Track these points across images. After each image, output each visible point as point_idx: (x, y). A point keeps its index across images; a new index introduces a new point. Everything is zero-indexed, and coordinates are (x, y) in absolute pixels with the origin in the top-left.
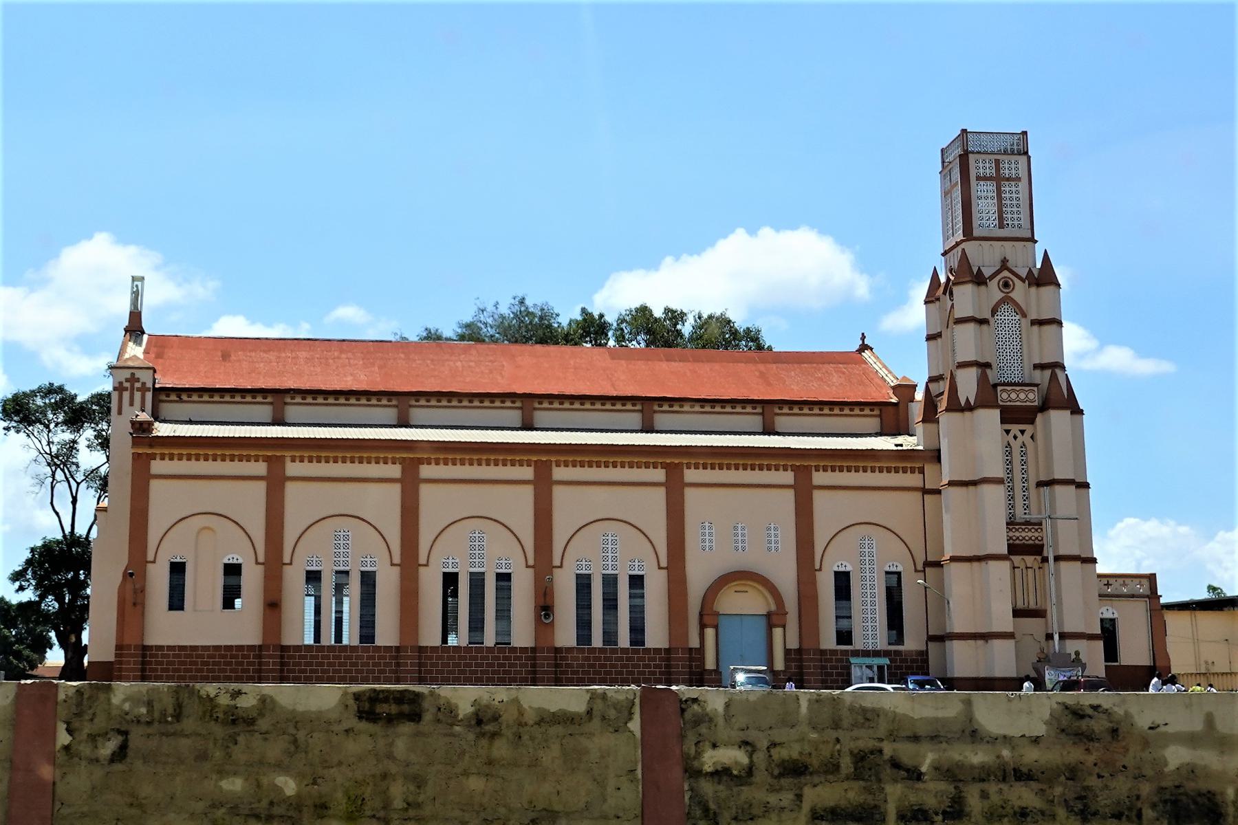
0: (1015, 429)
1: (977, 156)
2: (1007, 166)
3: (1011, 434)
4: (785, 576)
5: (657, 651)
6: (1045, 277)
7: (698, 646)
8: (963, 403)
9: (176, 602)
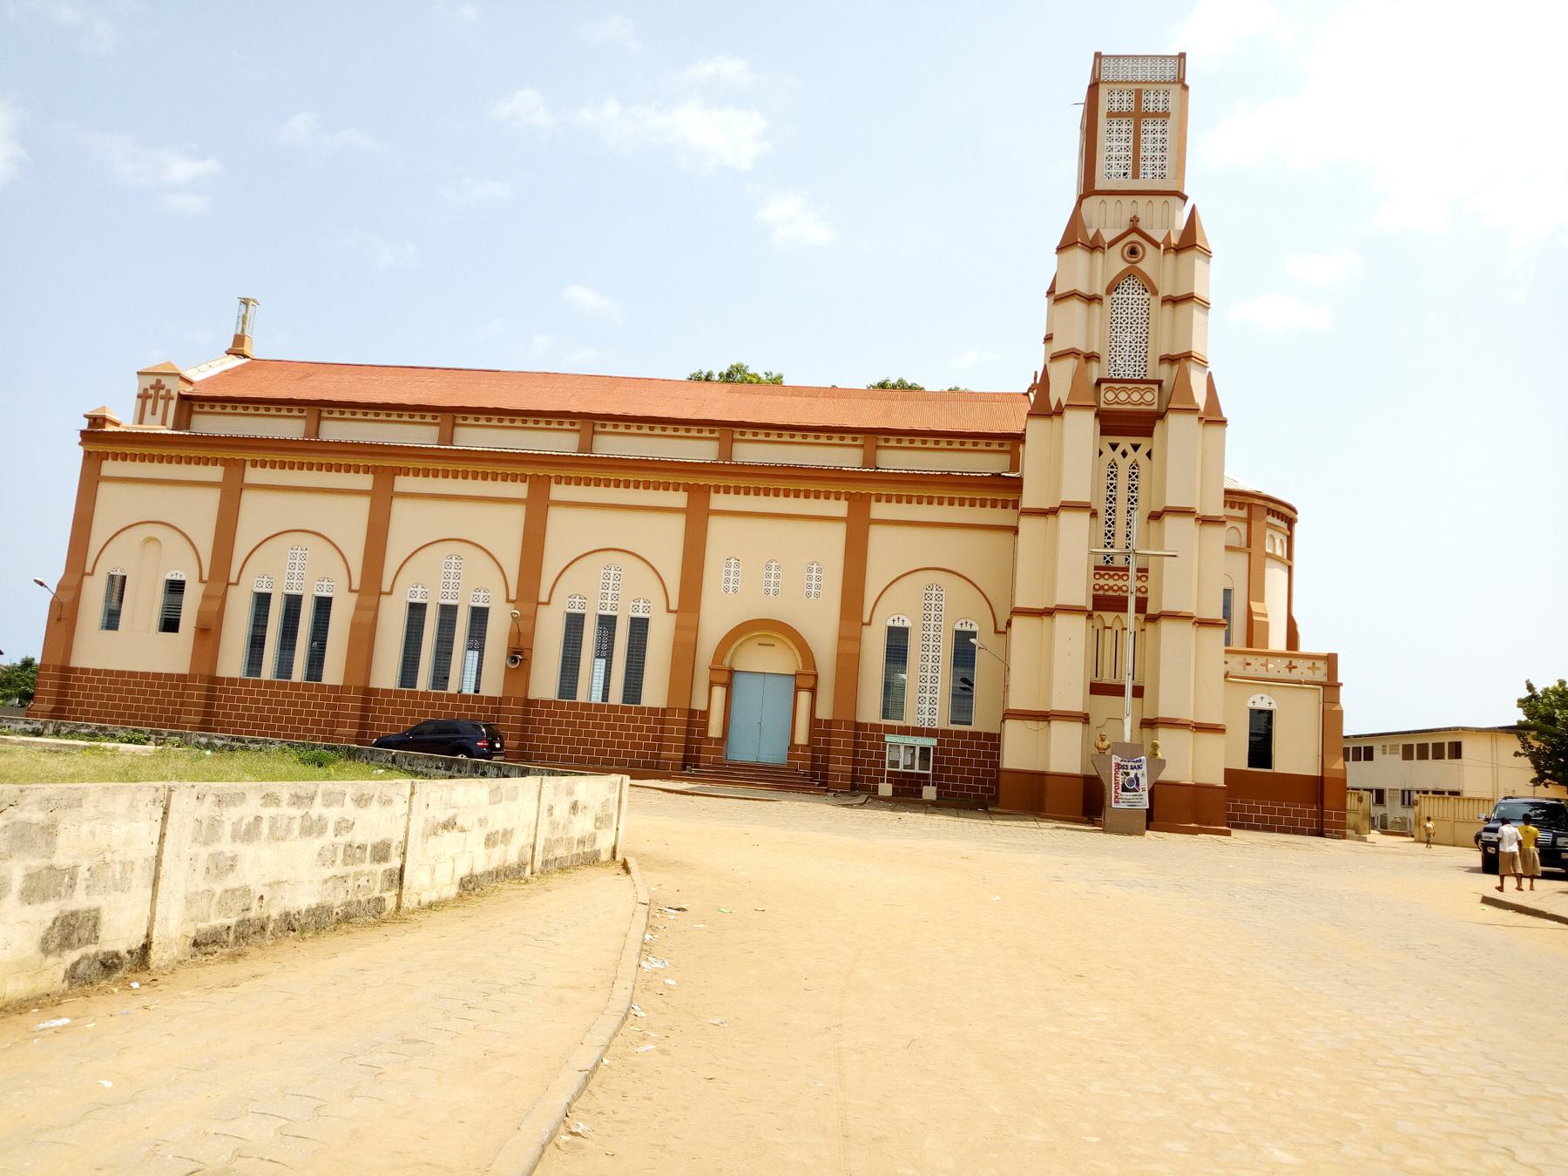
0: (1125, 443)
1: (1112, 86)
2: (1152, 97)
3: (1119, 450)
4: (822, 630)
5: (653, 711)
6: (1189, 241)
7: (704, 708)
8: (1053, 405)
9: (112, 620)
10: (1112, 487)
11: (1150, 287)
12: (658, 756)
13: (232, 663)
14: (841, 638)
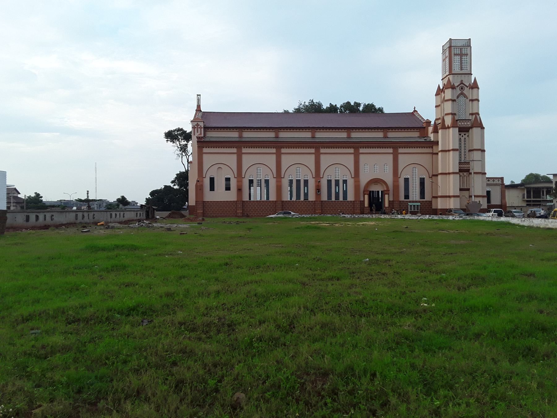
0: (463, 134)
1: (454, 47)
2: (464, 50)
3: (461, 135)
5: (351, 201)
6: (475, 86)
7: (363, 200)
8: (446, 126)
9: (212, 188)
10: (460, 144)
11: (465, 96)
12: (236, 212)
13: (324, 197)
14: (394, 181)
